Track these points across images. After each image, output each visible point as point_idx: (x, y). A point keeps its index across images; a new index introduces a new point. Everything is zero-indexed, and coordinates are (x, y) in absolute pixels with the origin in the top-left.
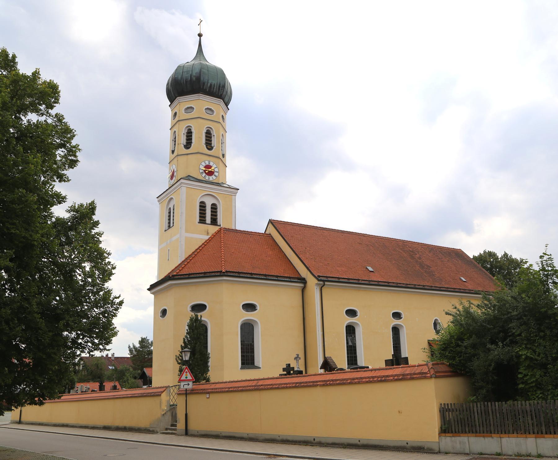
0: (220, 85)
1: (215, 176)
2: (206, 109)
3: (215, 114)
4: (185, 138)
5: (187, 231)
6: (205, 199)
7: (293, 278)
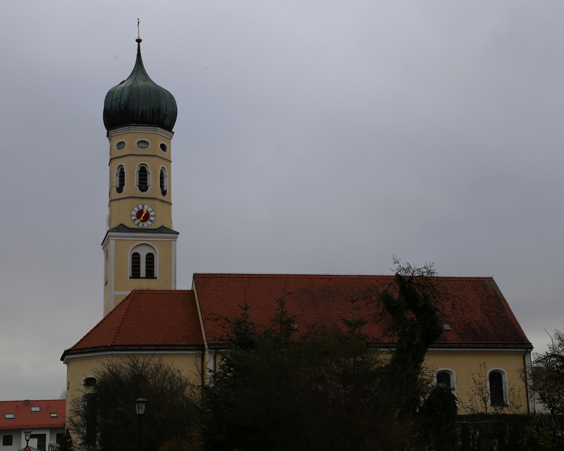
0: (154, 110)
1: (151, 221)
2: (138, 142)
3: (149, 146)
4: (118, 179)
5: (116, 289)
6: (139, 250)
7: (190, 346)
